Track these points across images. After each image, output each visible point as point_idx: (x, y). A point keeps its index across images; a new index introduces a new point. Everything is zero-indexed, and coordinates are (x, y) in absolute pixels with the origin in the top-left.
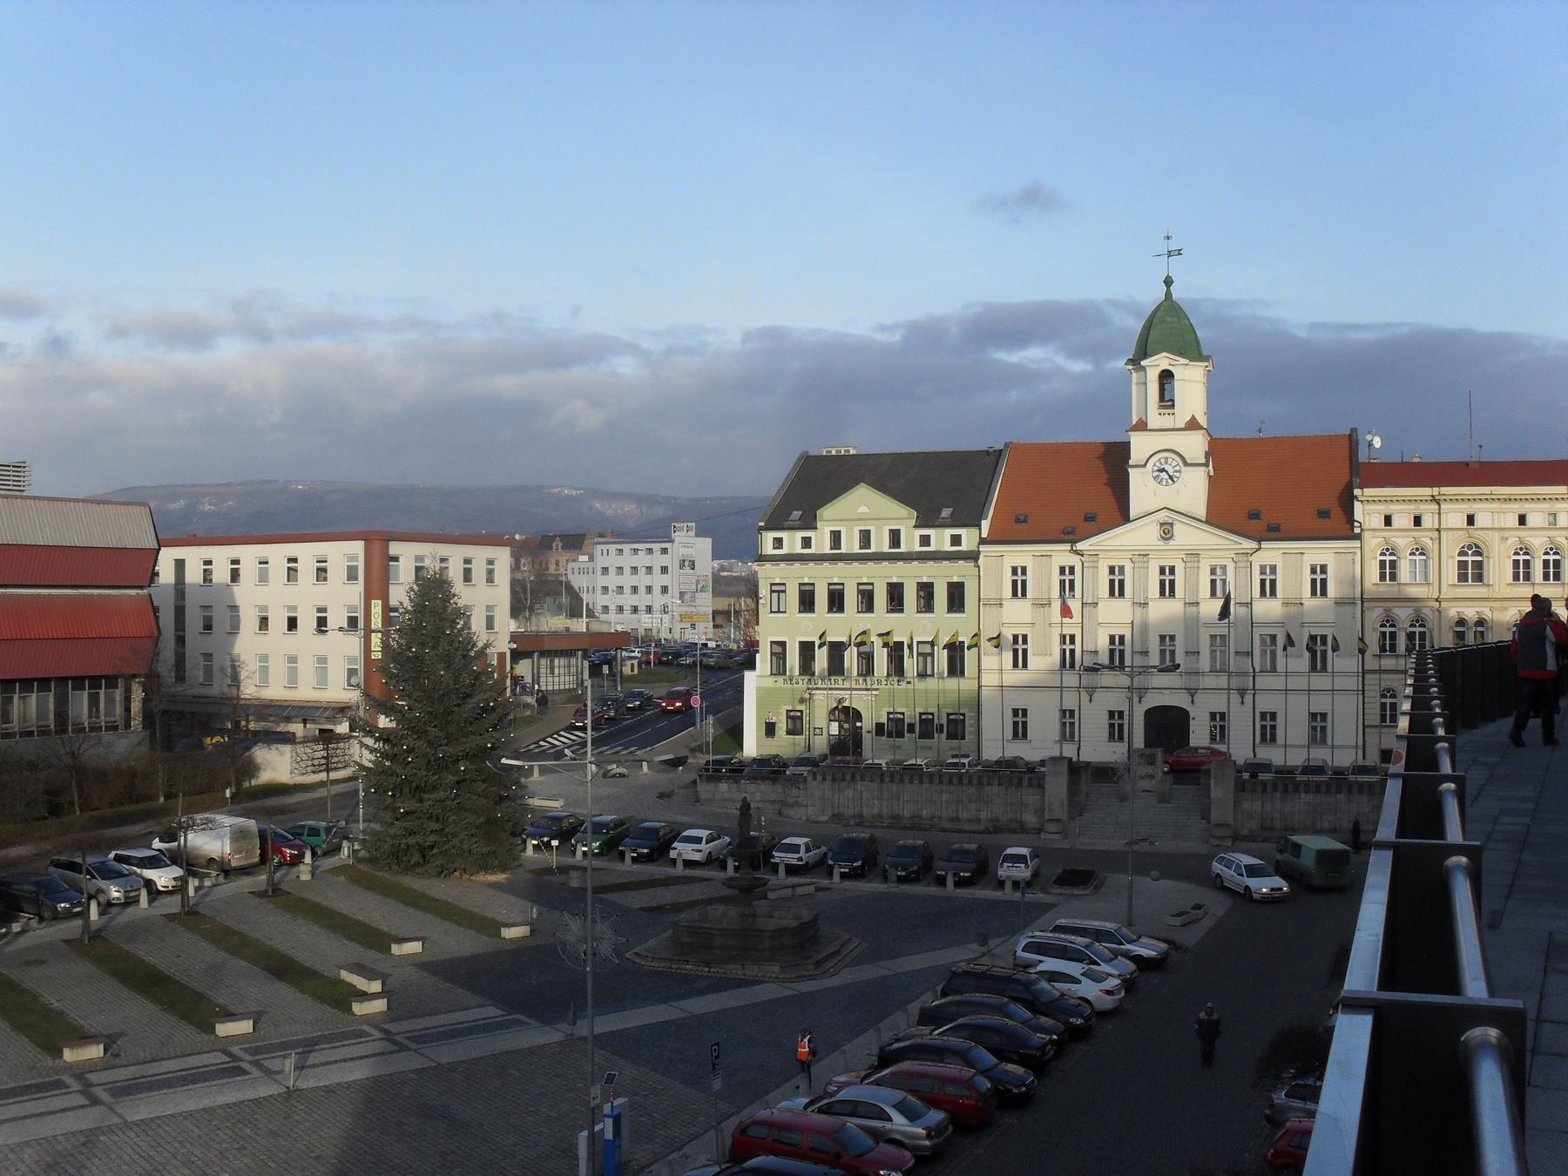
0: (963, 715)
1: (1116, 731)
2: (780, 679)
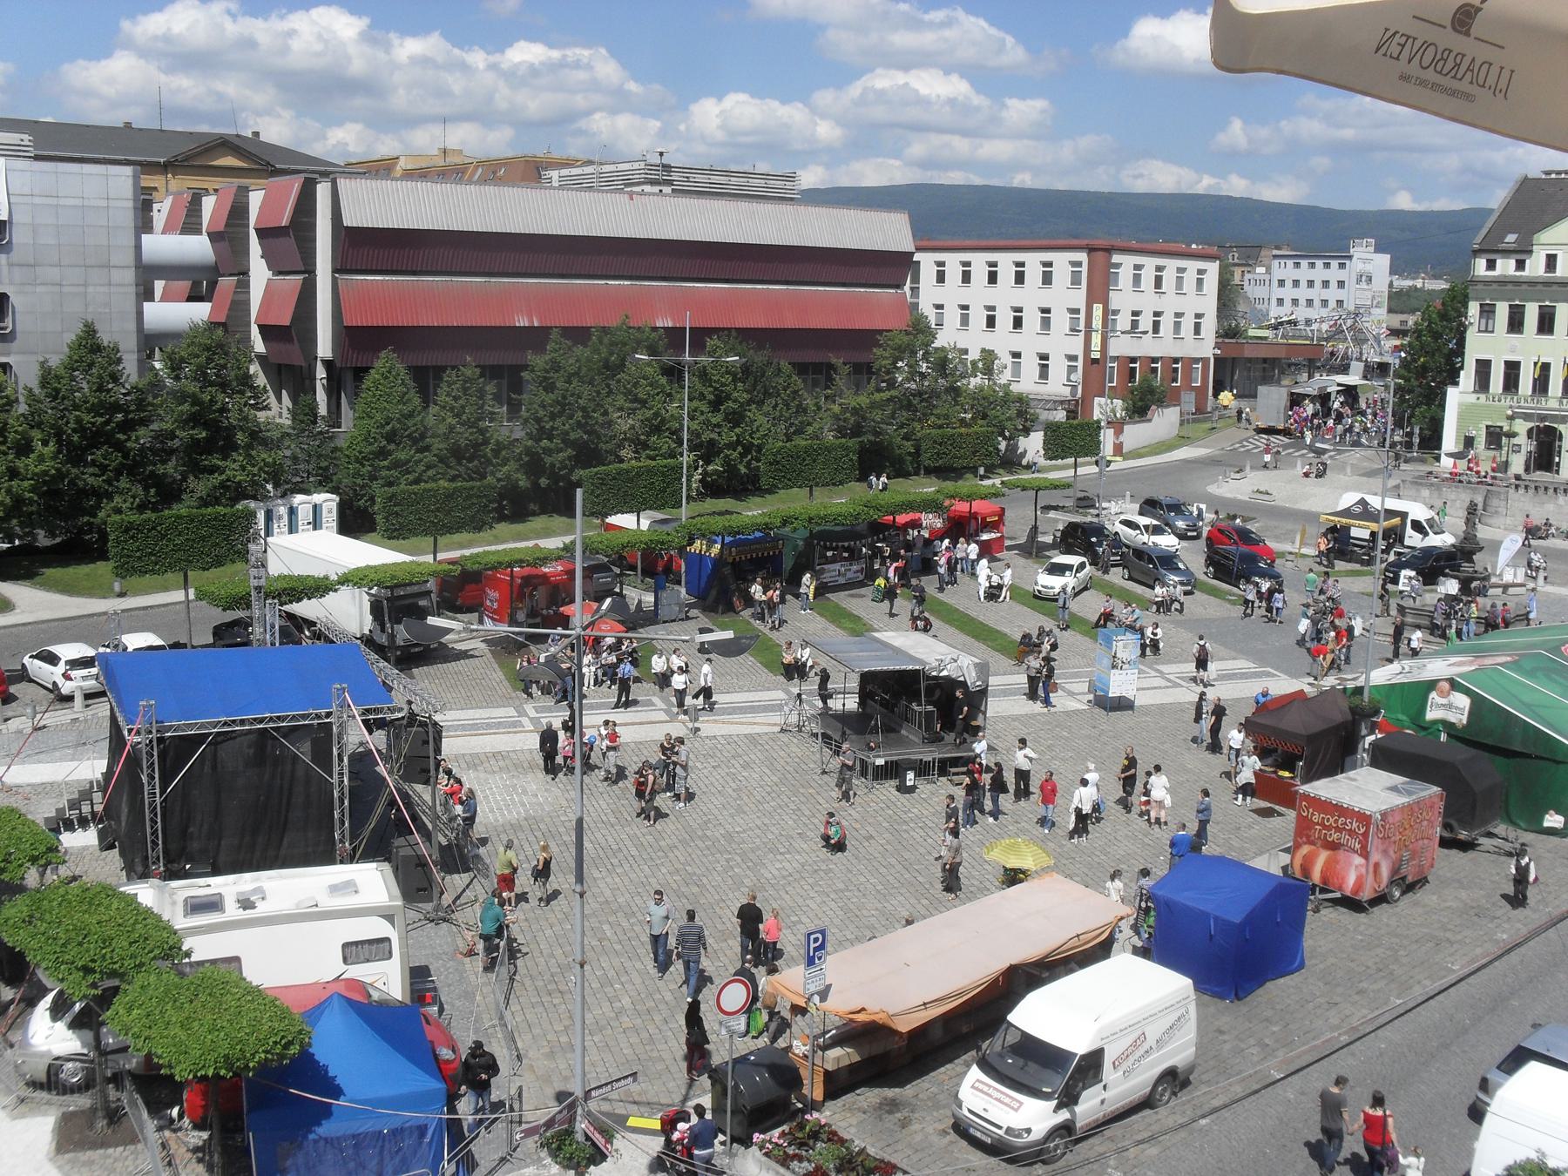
2: (1483, 397)
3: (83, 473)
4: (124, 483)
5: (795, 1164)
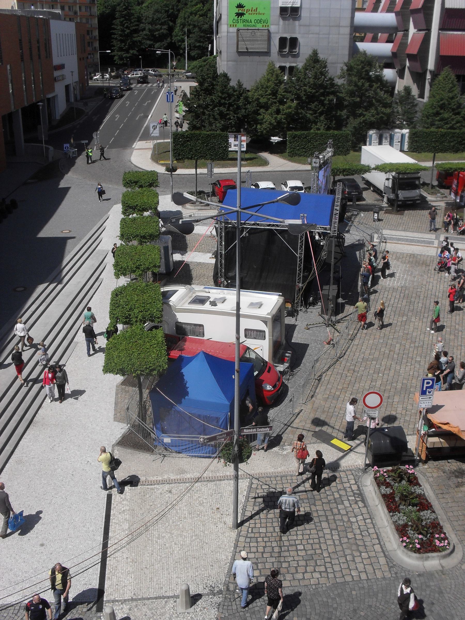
3: (306, 113)
4: (322, 118)
5: (383, 488)
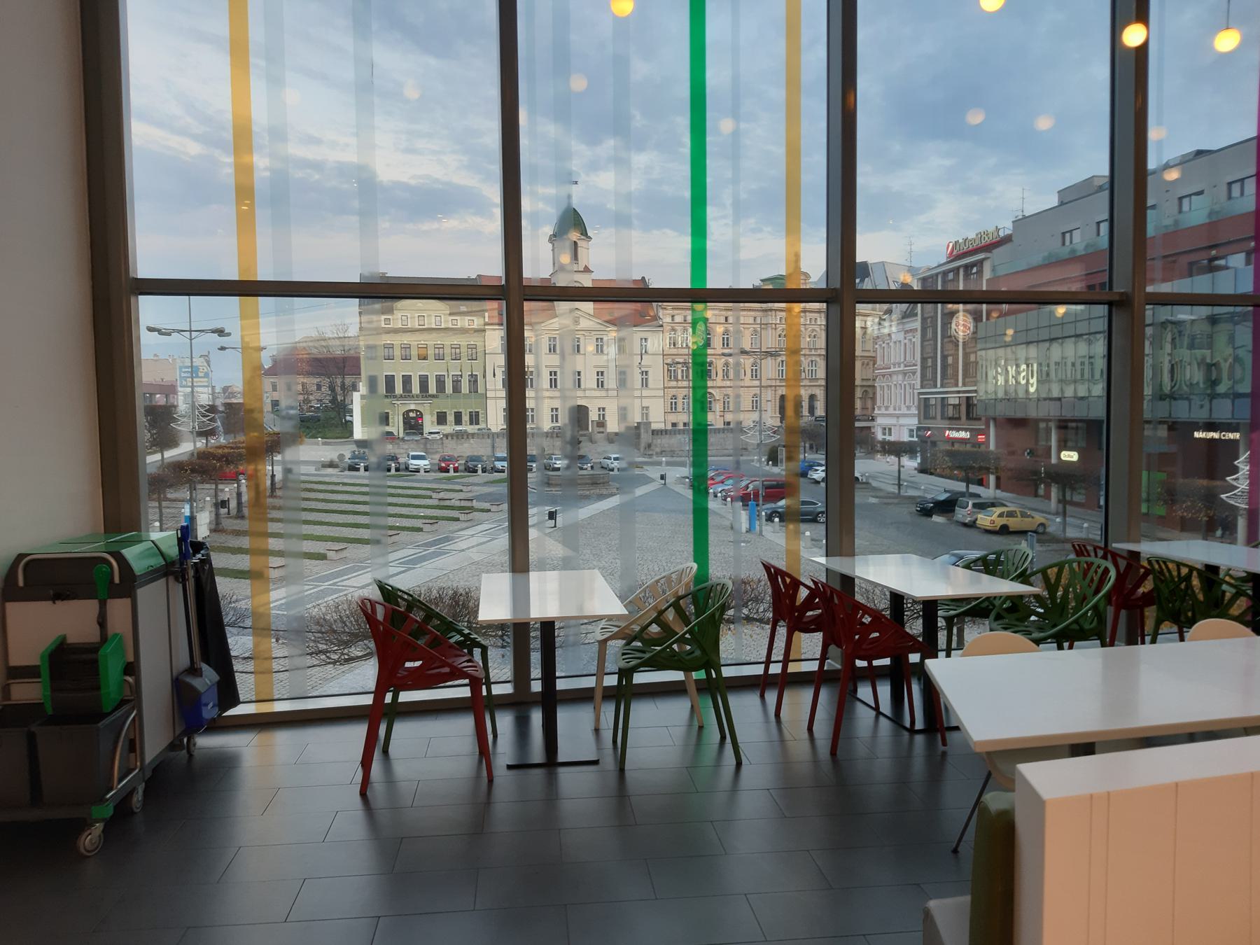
0: (478, 412)
1: (555, 418)
